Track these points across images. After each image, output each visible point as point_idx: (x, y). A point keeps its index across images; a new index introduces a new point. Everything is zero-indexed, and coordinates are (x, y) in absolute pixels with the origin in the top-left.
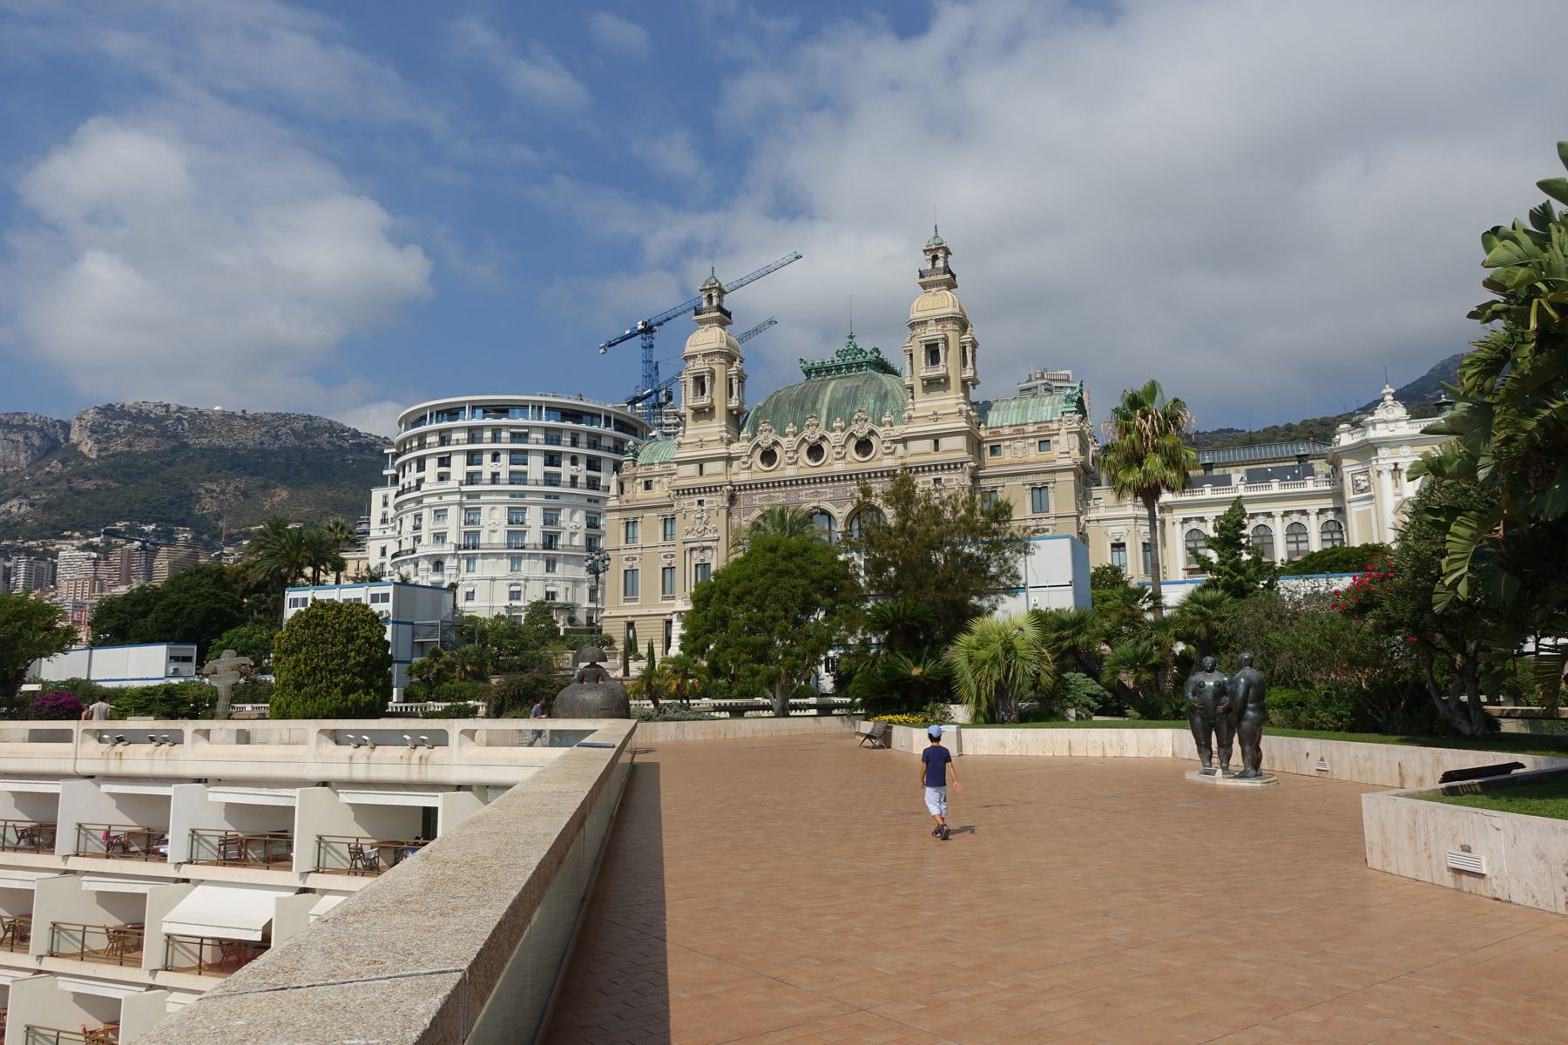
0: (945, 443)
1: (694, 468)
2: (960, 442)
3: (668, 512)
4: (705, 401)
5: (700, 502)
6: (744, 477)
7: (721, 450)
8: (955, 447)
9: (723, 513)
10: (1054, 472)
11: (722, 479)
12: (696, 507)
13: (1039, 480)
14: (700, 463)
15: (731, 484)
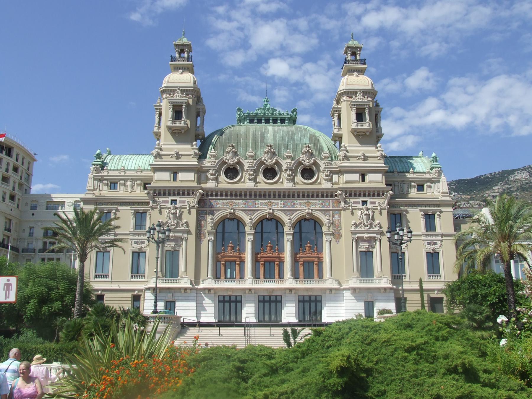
0: (369, 177)
1: (167, 175)
2: (379, 177)
3: (141, 208)
4: (181, 124)
5: (174, 201)
6: (211, 185)
7: (194, 162)
8: (376, 180)
9: (194, 212)
10: (438, 205)
11: (195, 184)
12: (169, 205)
13: (430, 210)
14: (175, 172)
15: (202, 189)
